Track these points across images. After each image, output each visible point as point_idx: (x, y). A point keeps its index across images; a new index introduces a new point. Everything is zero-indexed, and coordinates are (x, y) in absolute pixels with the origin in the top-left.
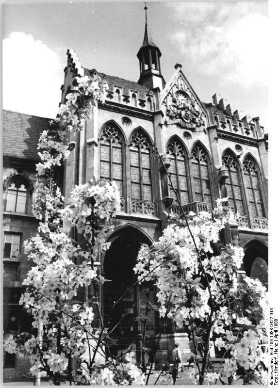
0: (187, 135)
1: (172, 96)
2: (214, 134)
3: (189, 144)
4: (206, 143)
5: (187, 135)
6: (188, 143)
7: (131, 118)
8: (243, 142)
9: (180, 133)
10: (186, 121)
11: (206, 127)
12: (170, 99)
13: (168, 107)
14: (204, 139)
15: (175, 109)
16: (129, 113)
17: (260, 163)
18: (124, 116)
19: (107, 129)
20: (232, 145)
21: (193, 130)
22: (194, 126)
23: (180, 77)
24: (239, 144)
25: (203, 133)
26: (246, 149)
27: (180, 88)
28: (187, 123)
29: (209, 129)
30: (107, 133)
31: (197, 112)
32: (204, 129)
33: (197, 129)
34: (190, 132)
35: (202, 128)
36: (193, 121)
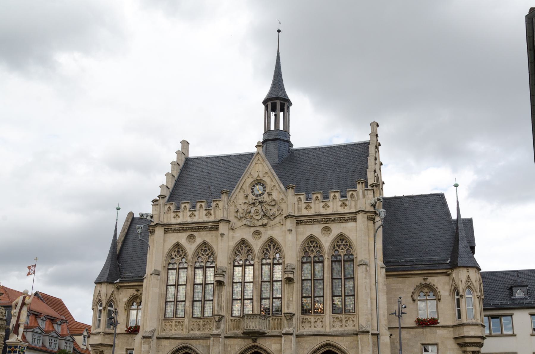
0: (257, 233)
1: (244, 192)
5: (257, 233)
6: (257, 245)
7: (195, 234)
8: (334, 221)
9: (247, 234)
10: (258, 218)
12: (241, 196)
13: (239, 207)
14: (276, 232)
15: (245, 207)
16: (191, 228)
17: (355, 244)
18: (190, 233)
21: (264, 225)
23: (259, 162)
24: (326, 225)
26: (336, 229)
27: (255, 176)
29: (285, 217)
30: (173, 256)
31: (274, 200)
33: (272, 223)
34: (261, 229)
35: (277, 219)
36: (265, 215)
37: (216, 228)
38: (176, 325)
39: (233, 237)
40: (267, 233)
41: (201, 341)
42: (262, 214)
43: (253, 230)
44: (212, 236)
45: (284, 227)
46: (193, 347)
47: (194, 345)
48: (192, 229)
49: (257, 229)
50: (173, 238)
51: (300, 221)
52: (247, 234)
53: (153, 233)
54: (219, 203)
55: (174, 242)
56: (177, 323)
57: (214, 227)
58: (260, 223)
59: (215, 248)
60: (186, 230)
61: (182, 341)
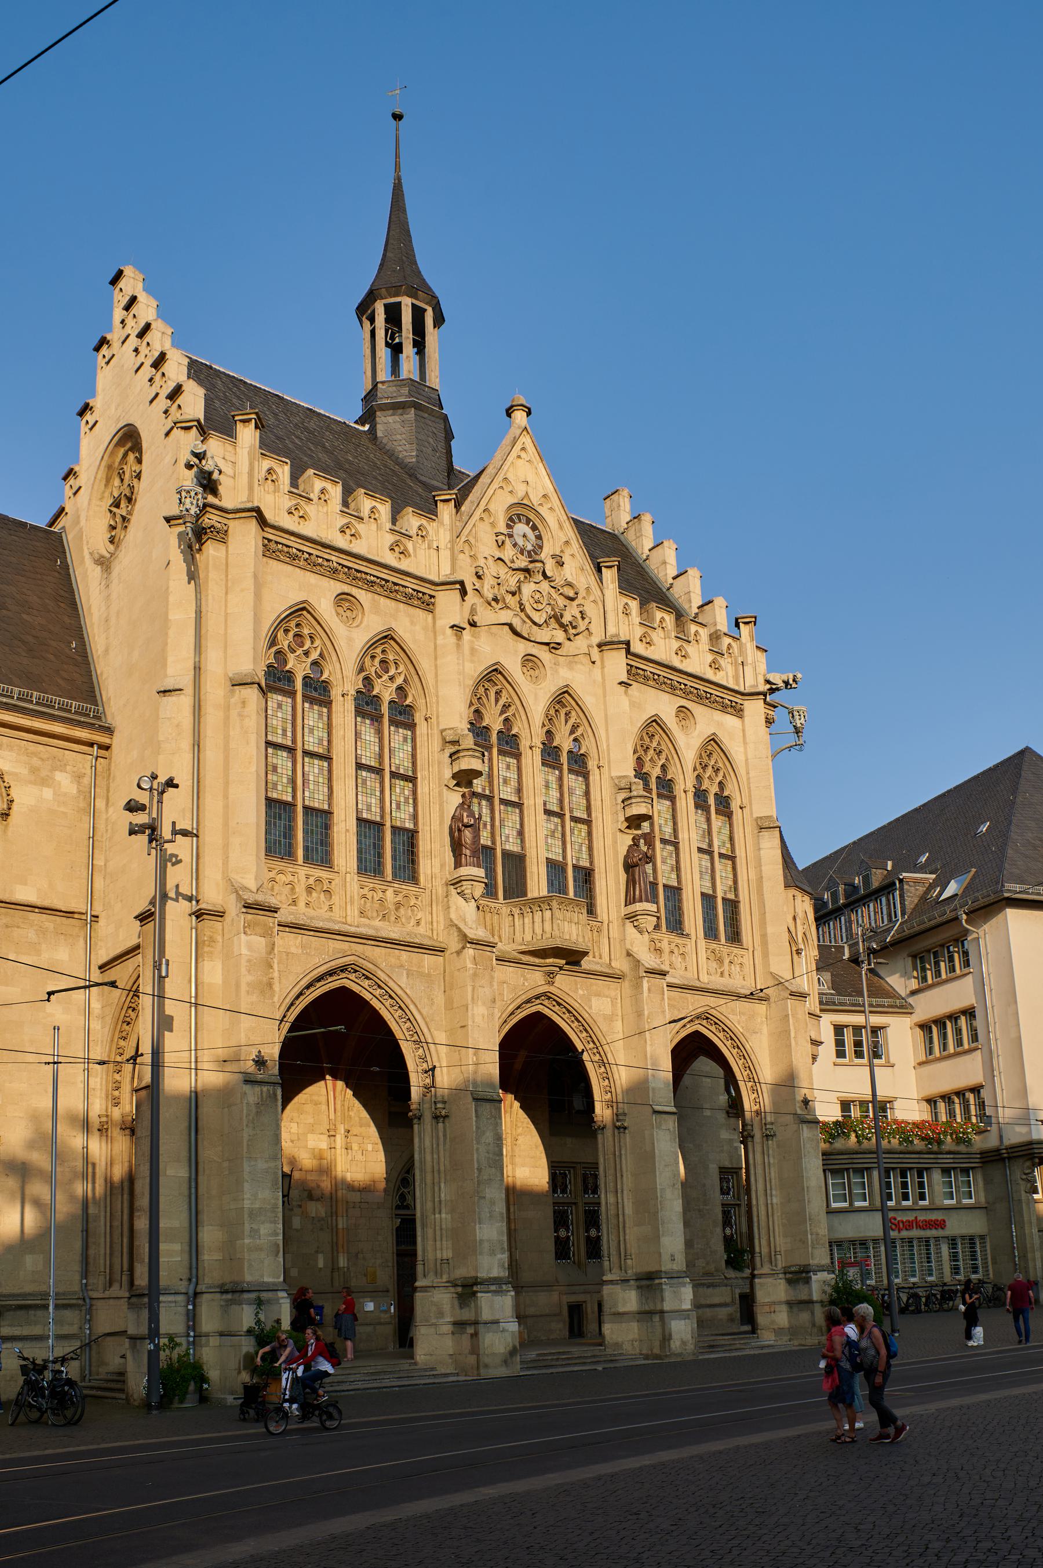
2: (617, 663)
3: (536, 698)
4: (589, 701)
9: (510, 655)
11: (596, 640)
14: (580, 679)
15: (503, 571)
19: (286, 631)
20: (664, 705)
22: (559, 636)
25: (586, 660)
28: (535, 623)
32: (590, 646)
35: (580, 644)
37: (427, 604)
38: (309, 889)
39: (473, 651)
40: (558, 674)
41: (404, 956)
42: (549, 609)
43: (523, 648)
44: (412, 623)
45: (597, 671)
46: (380, 974)
47: (383, 965)
48: (354, 577)
49: (535, 650)
50: (291, 585)
51: (642, 671)
52: (510, 655)
53: (222, 536)
54: (431, 527)
55: (295, 597)
56: (311, 881)
57: (420, 596)
58: (544, 635)
59: (425, 664)
60: (333, 573)
61: (339, 945)
